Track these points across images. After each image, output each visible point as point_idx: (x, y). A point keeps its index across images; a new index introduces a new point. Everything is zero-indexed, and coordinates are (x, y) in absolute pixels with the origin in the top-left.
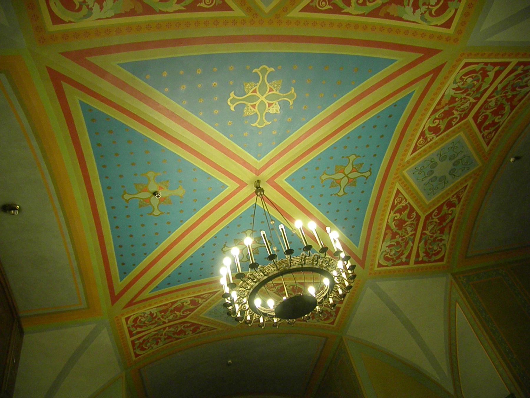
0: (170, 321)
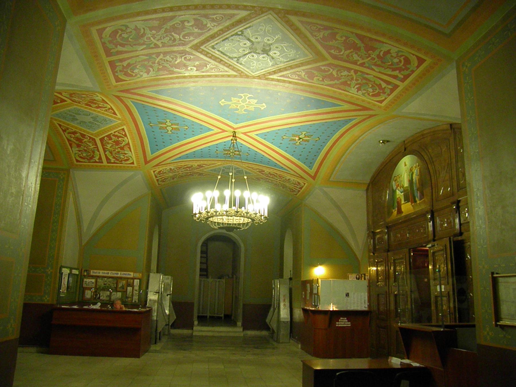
0: (181, 171)
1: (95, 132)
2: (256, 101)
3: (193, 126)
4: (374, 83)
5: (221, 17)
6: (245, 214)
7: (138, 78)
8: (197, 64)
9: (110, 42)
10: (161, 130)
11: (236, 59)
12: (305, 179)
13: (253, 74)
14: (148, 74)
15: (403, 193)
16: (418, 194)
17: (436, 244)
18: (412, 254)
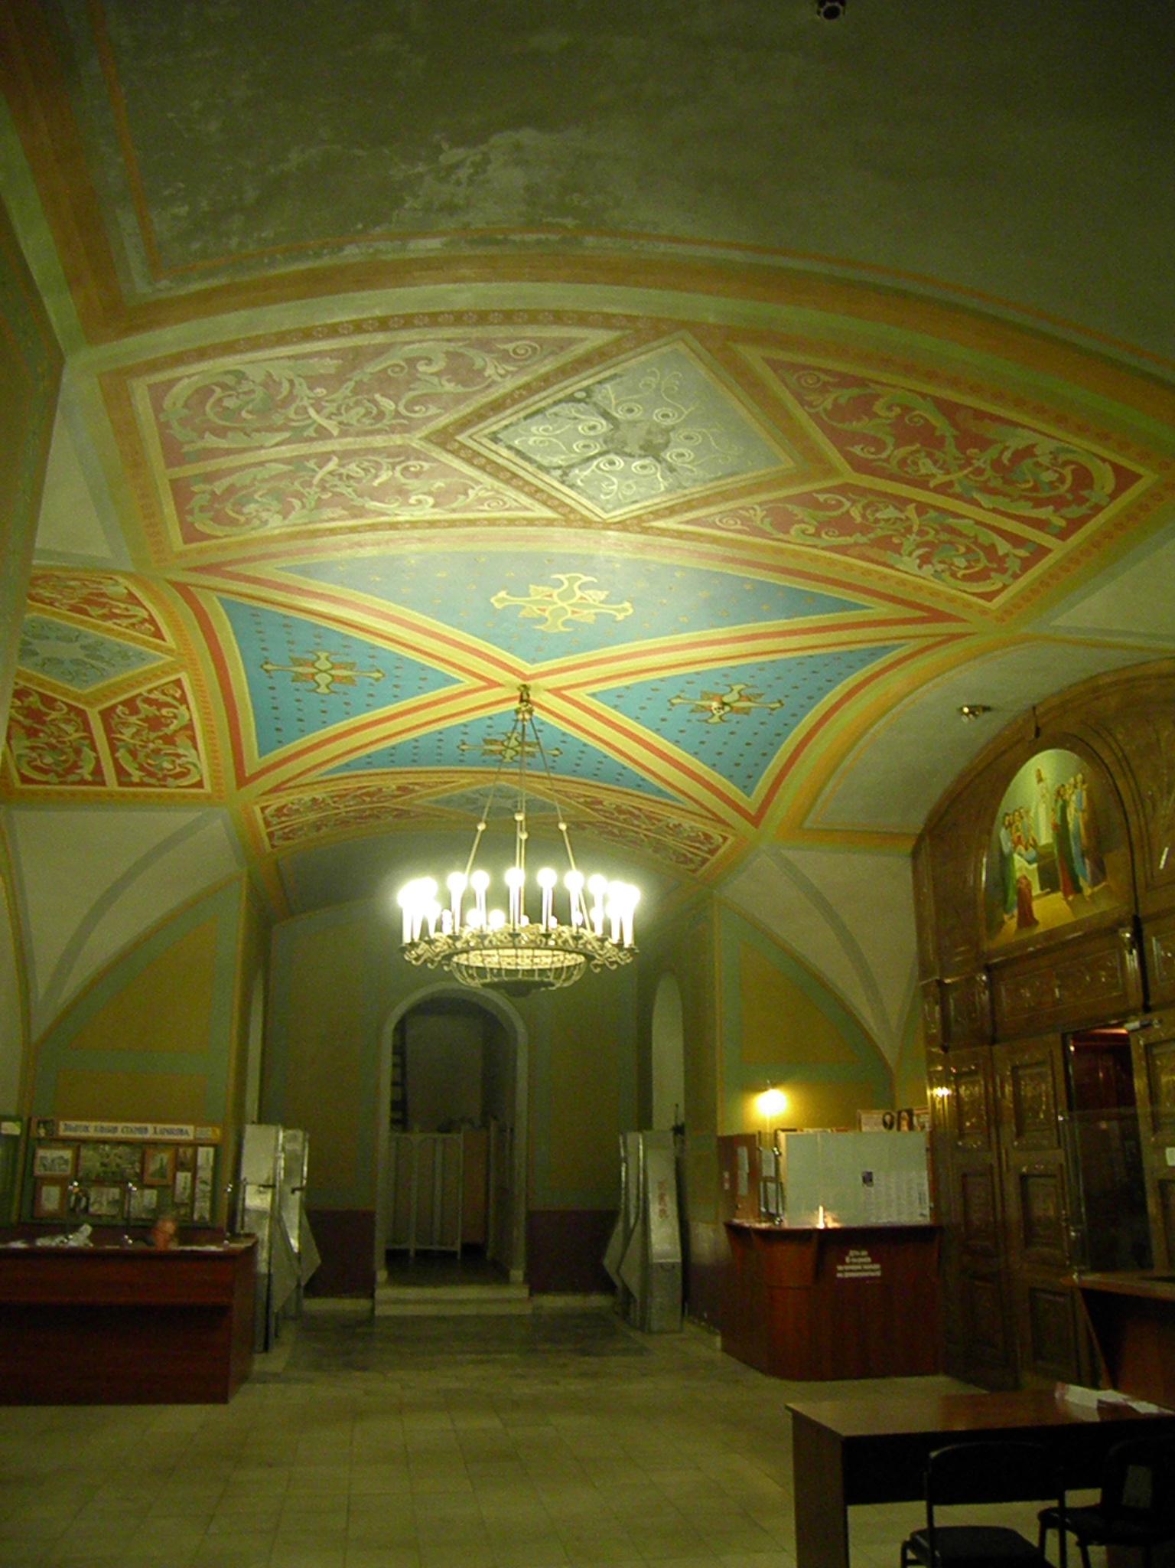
0: (346, 806)
1: (87, 691)
2: (602, 595)
3: (398, 672)
4: (976, 543)
5: (531, 346)
6: (571, 941)
7: (253, 529)
8: (439, 488)
9: (184, 422)
10: (298, 685)
11: (559, 472)
12: (728, 825)
13: (605, 516)
14: (285, 518)
15: (1035, 865)
16: (1084, 870)
17: (1156, 1021)
18: (1072, 1048)
